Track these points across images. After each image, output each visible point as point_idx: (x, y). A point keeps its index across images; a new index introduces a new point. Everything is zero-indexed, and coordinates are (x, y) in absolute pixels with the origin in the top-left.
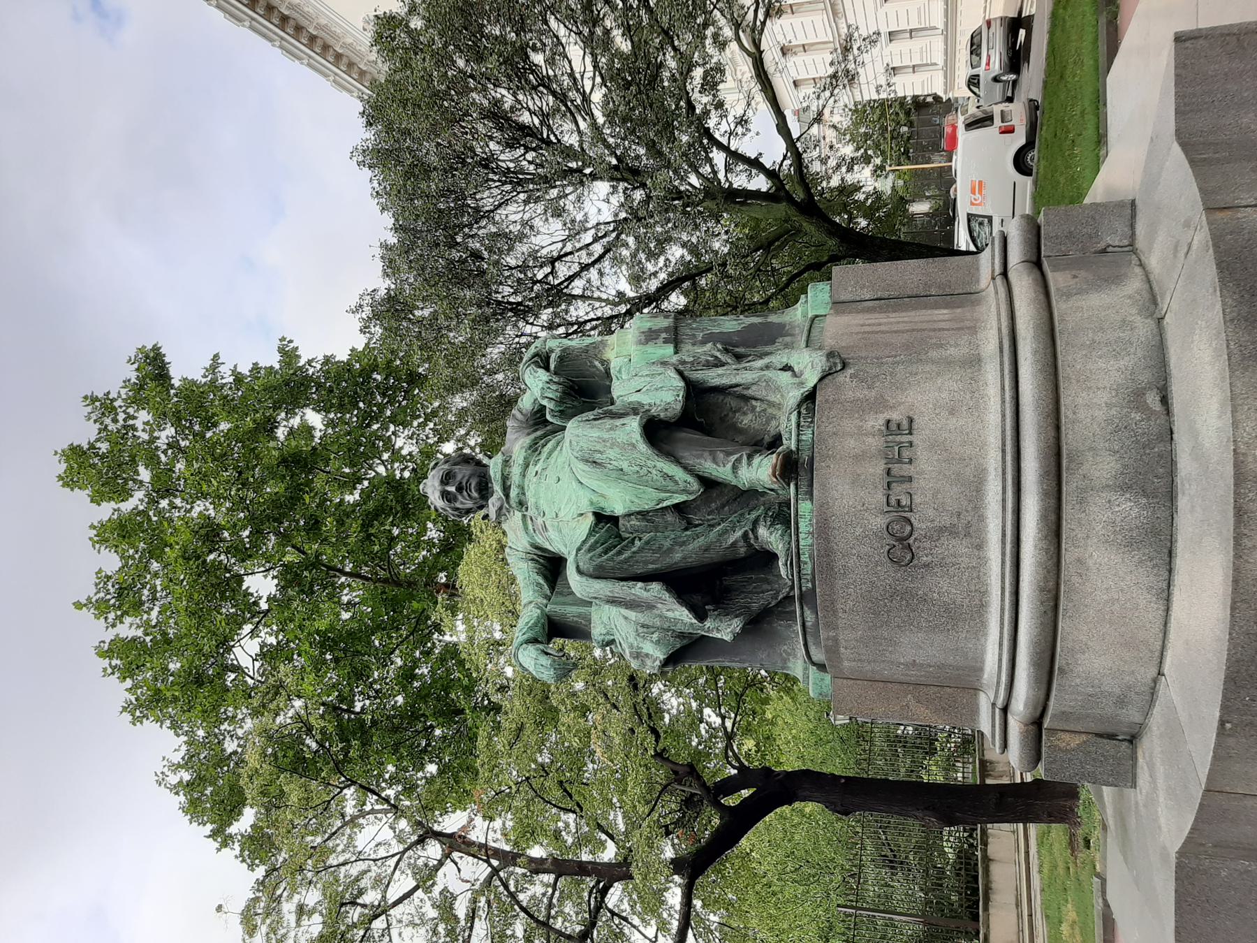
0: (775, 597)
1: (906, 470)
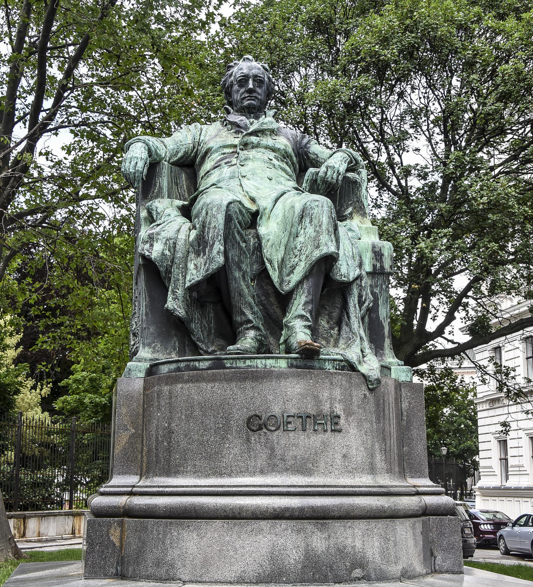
0: (199, 339)
1: (309, 427)
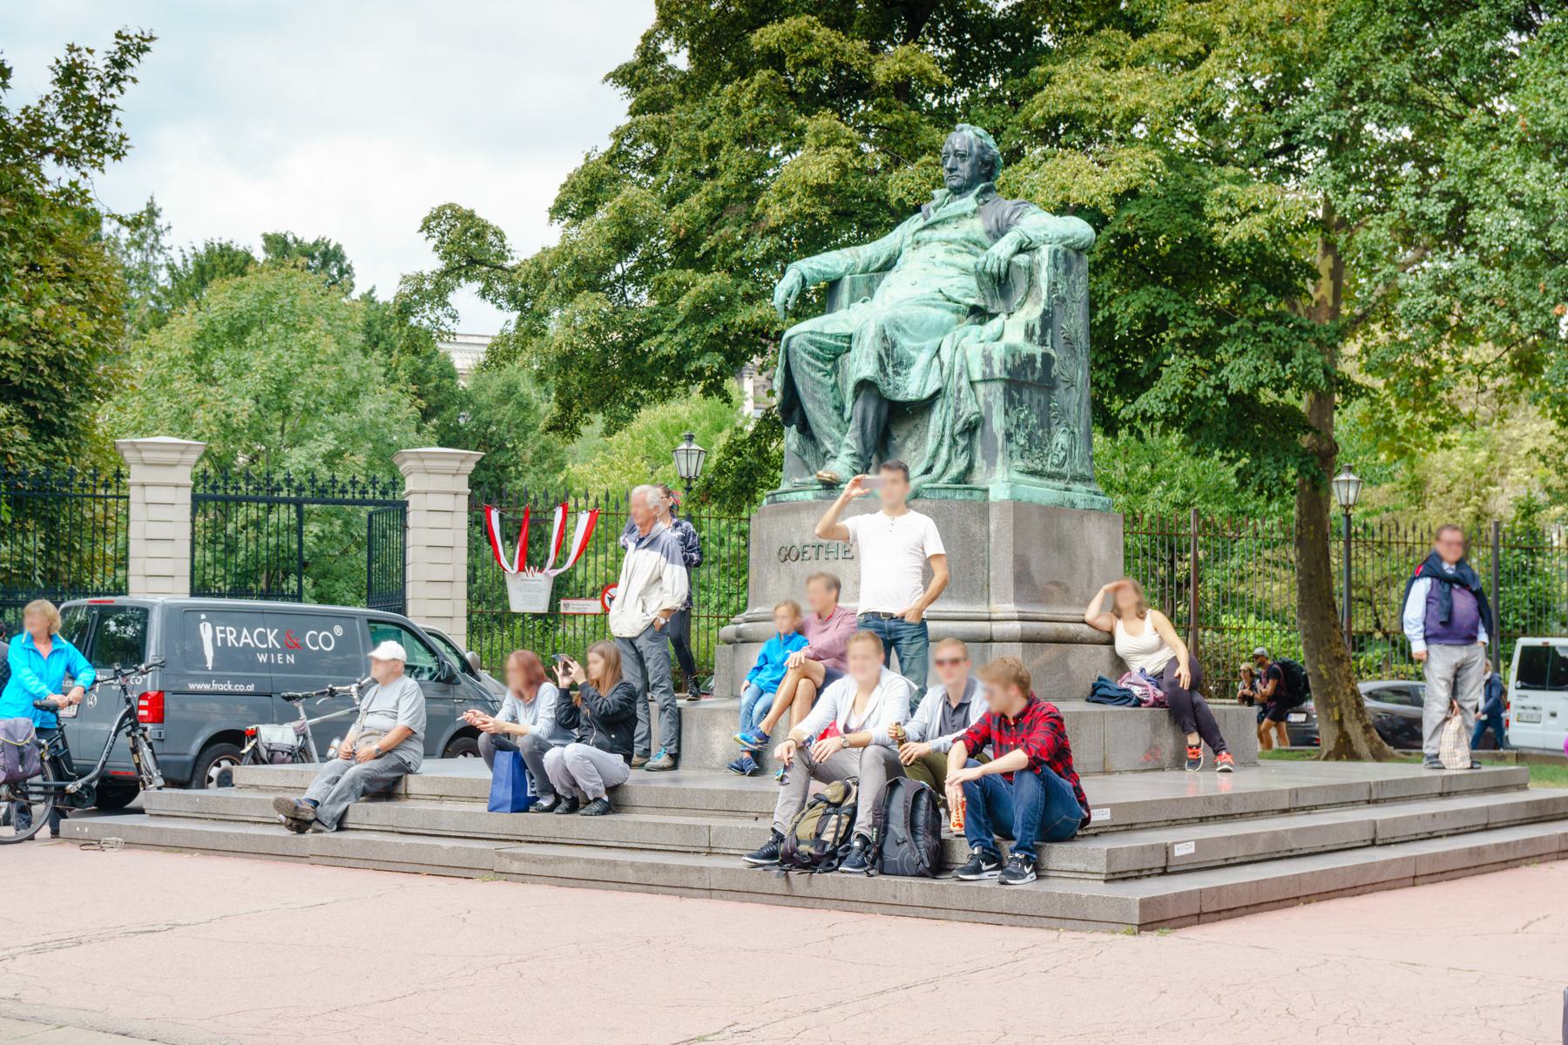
1: (822, 556)
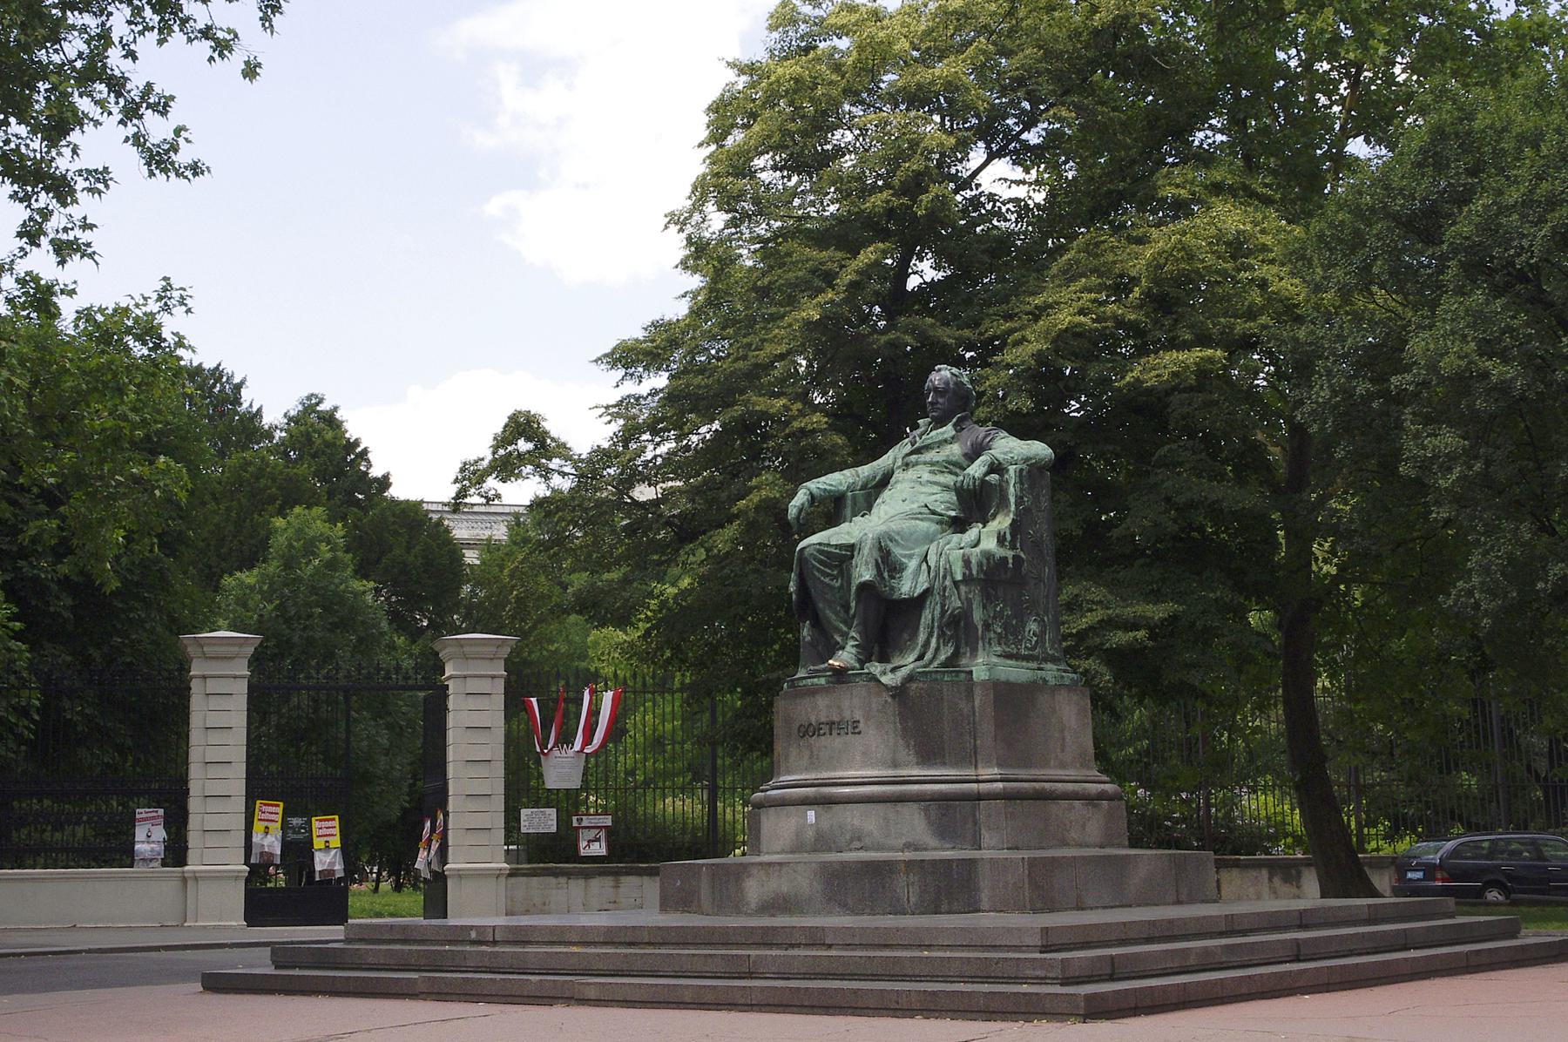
1: (835, 732)
